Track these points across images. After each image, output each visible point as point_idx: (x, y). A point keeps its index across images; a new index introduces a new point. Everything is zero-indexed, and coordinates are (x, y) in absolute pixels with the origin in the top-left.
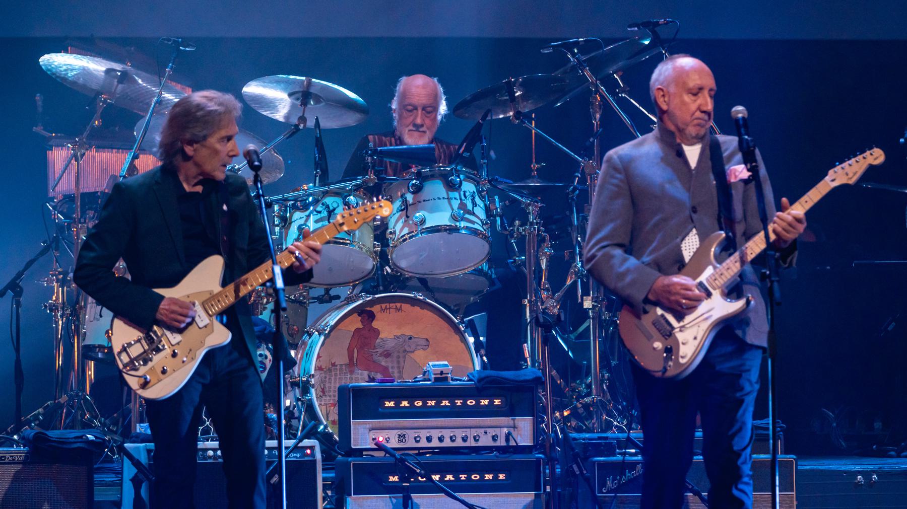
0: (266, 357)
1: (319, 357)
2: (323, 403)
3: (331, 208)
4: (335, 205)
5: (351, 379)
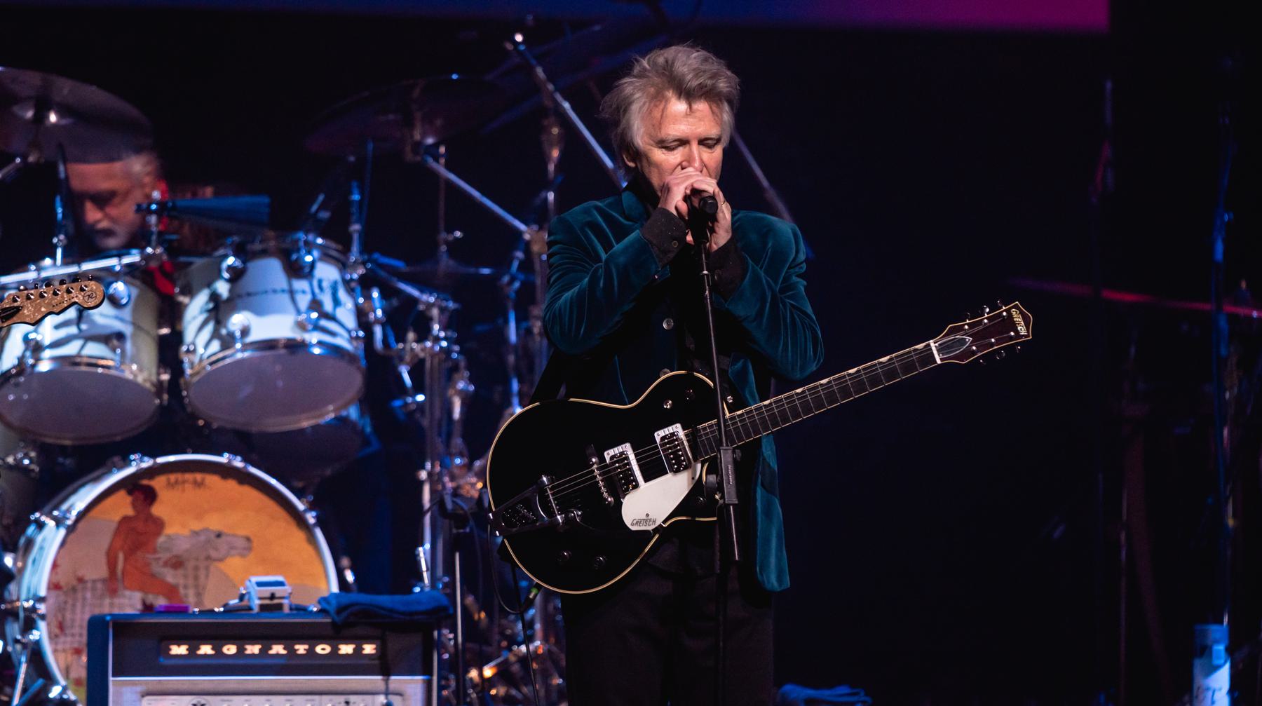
1: (55, 566)
2: (60, 647)
5: (112, 605)
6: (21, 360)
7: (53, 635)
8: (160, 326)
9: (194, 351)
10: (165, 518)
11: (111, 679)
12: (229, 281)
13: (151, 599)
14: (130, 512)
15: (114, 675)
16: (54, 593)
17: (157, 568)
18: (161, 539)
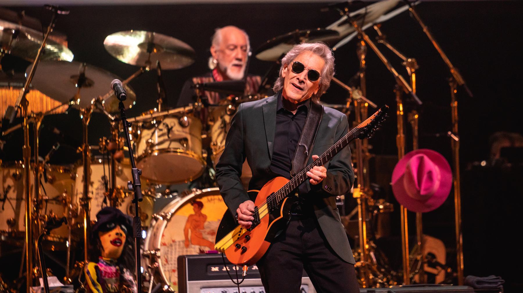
0: (121, 235)
1: (163, 236)
2: (167, 269)
3: (170, 127)
4: (172, 124)
5: (187, 251)
6: (146, 151)
7: (163, 265)
8: (202, 134)
9: (217, 144)
10: (207, 215)
11: (188, 282)
12: (230, 115)
13: (203, 248)
14: (193, 212)
15: (189, 280)
16: (163, 247)
17: (205, 236)
18: (206, 224)
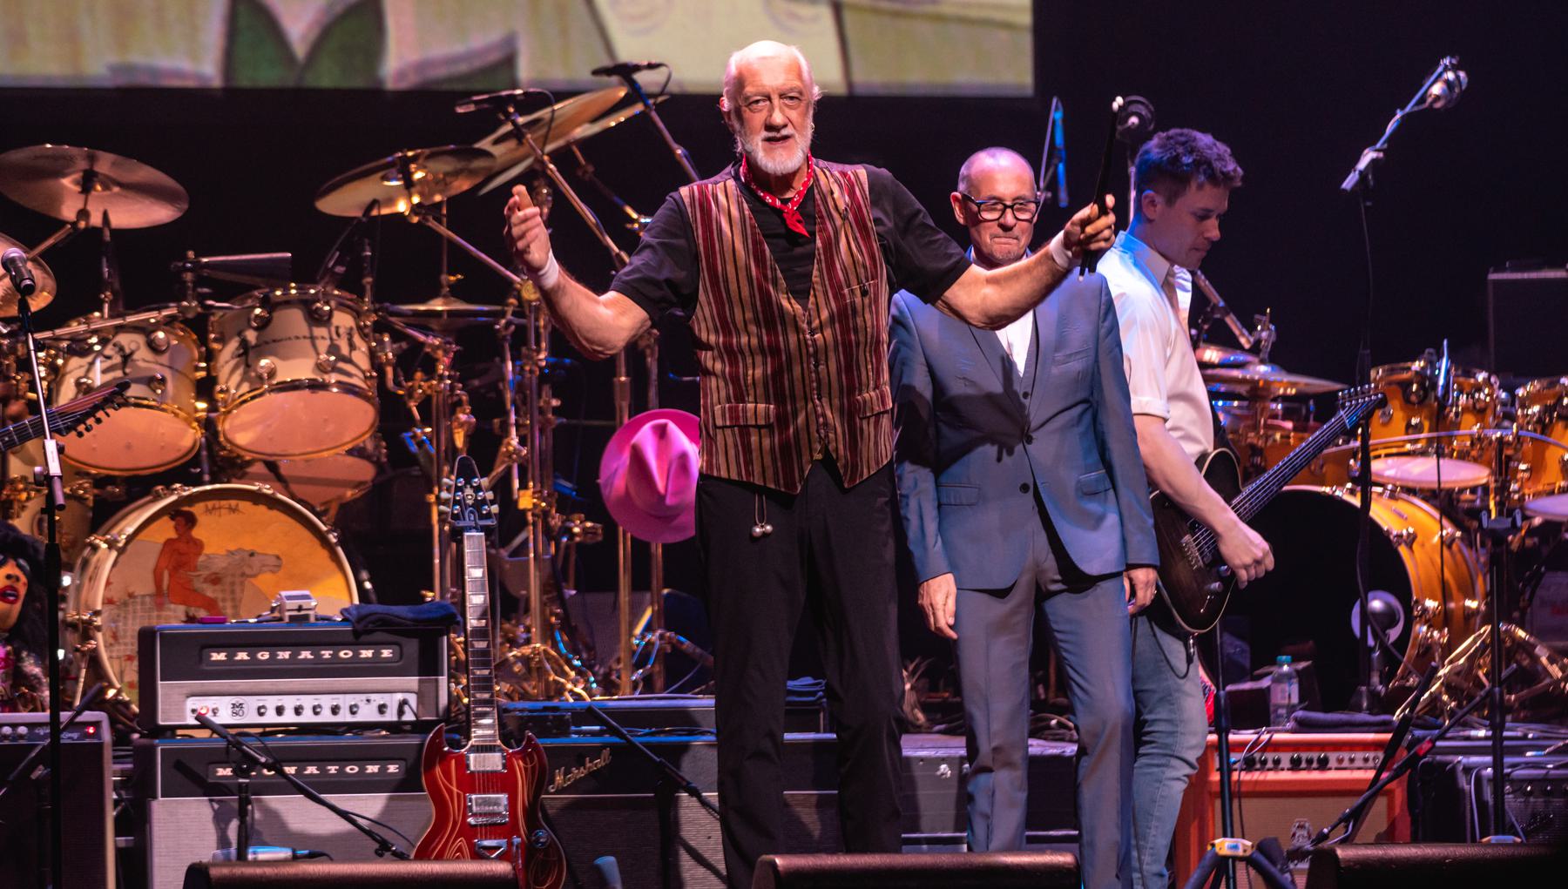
1: (108, 583)
2: (114, 655)
3: (128, 351)
4: (133, 346)
5: (159, 617)
13: (192, 611)
